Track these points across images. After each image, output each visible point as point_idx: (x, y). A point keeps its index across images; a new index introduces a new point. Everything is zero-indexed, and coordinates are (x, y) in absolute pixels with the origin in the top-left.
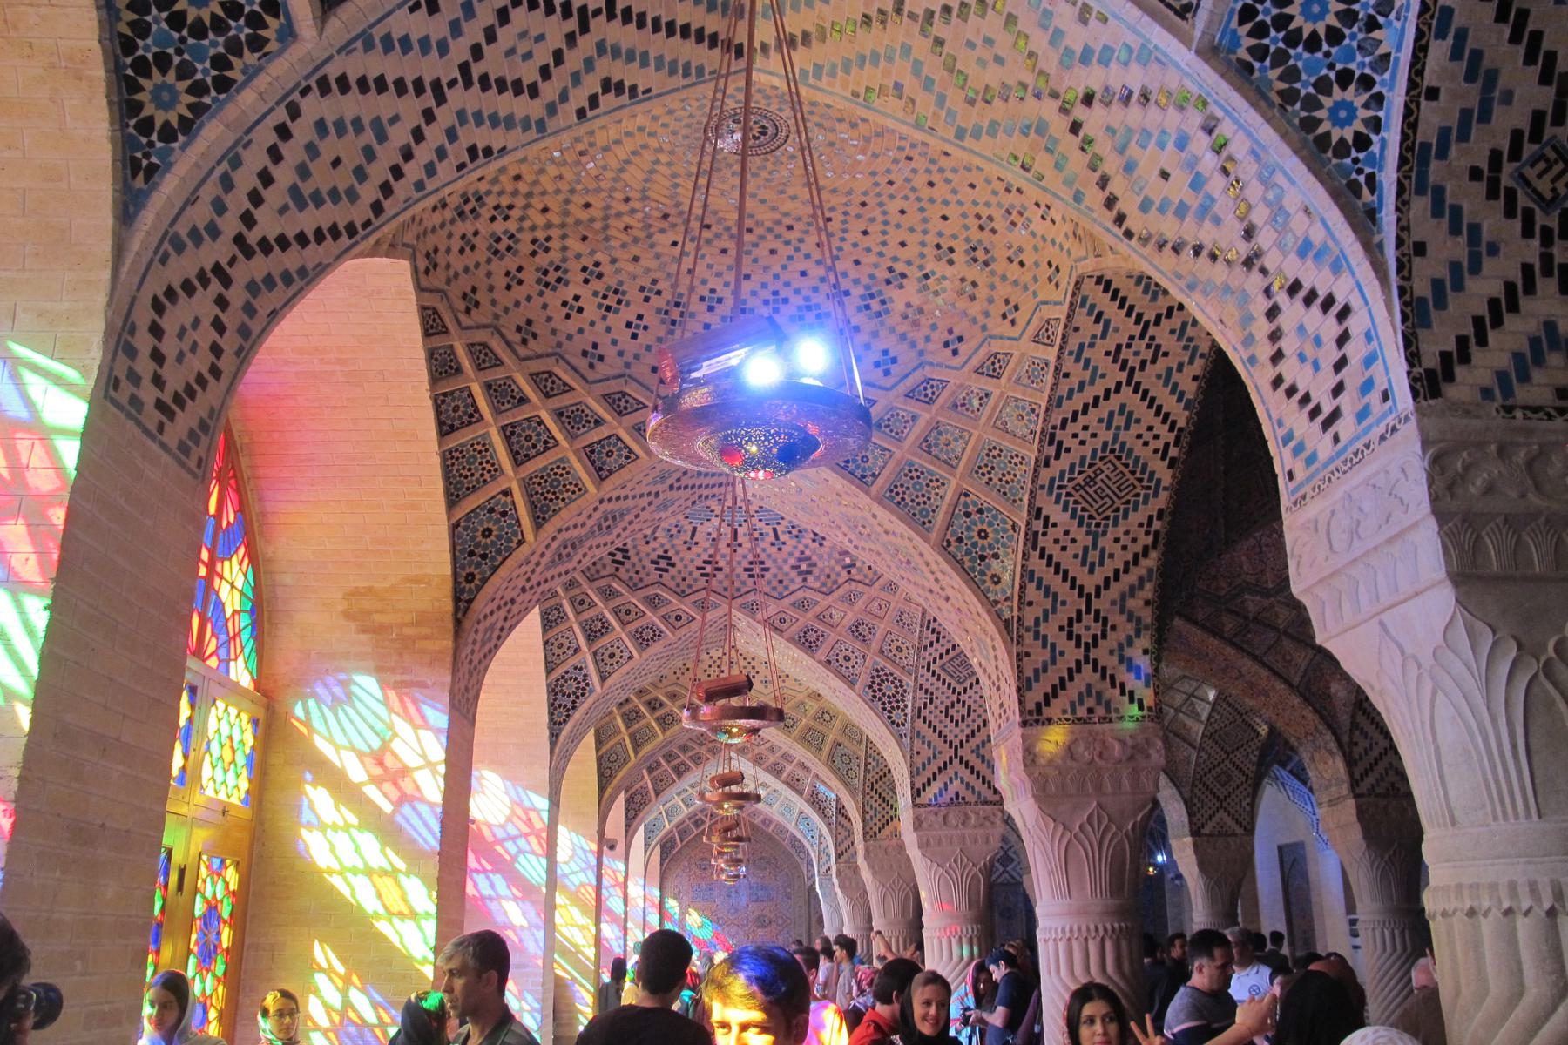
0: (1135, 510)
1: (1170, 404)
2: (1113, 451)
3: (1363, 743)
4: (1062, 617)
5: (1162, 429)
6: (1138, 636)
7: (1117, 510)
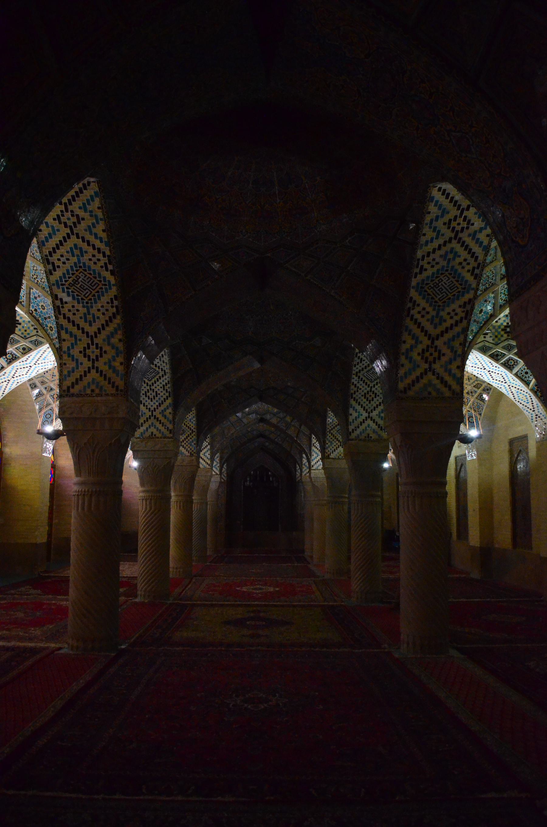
0: (103, 295)
1: (98, 243)
2: (80, 267)
3: (355, 415)
4: (81, 346)
5: (101, 256)
6: (118, 356)
7: (94, 295)
